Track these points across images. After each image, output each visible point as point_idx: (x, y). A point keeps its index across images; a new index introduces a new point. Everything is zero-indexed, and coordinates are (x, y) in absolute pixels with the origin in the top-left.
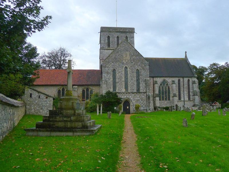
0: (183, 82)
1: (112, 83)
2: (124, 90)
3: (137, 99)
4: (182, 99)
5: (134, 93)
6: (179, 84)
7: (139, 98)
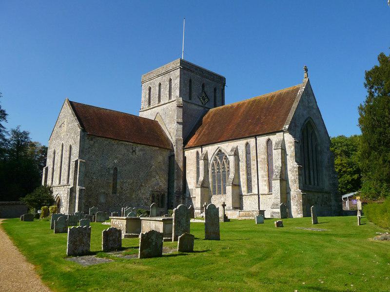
4: (255, 191)
6: (248, 153)
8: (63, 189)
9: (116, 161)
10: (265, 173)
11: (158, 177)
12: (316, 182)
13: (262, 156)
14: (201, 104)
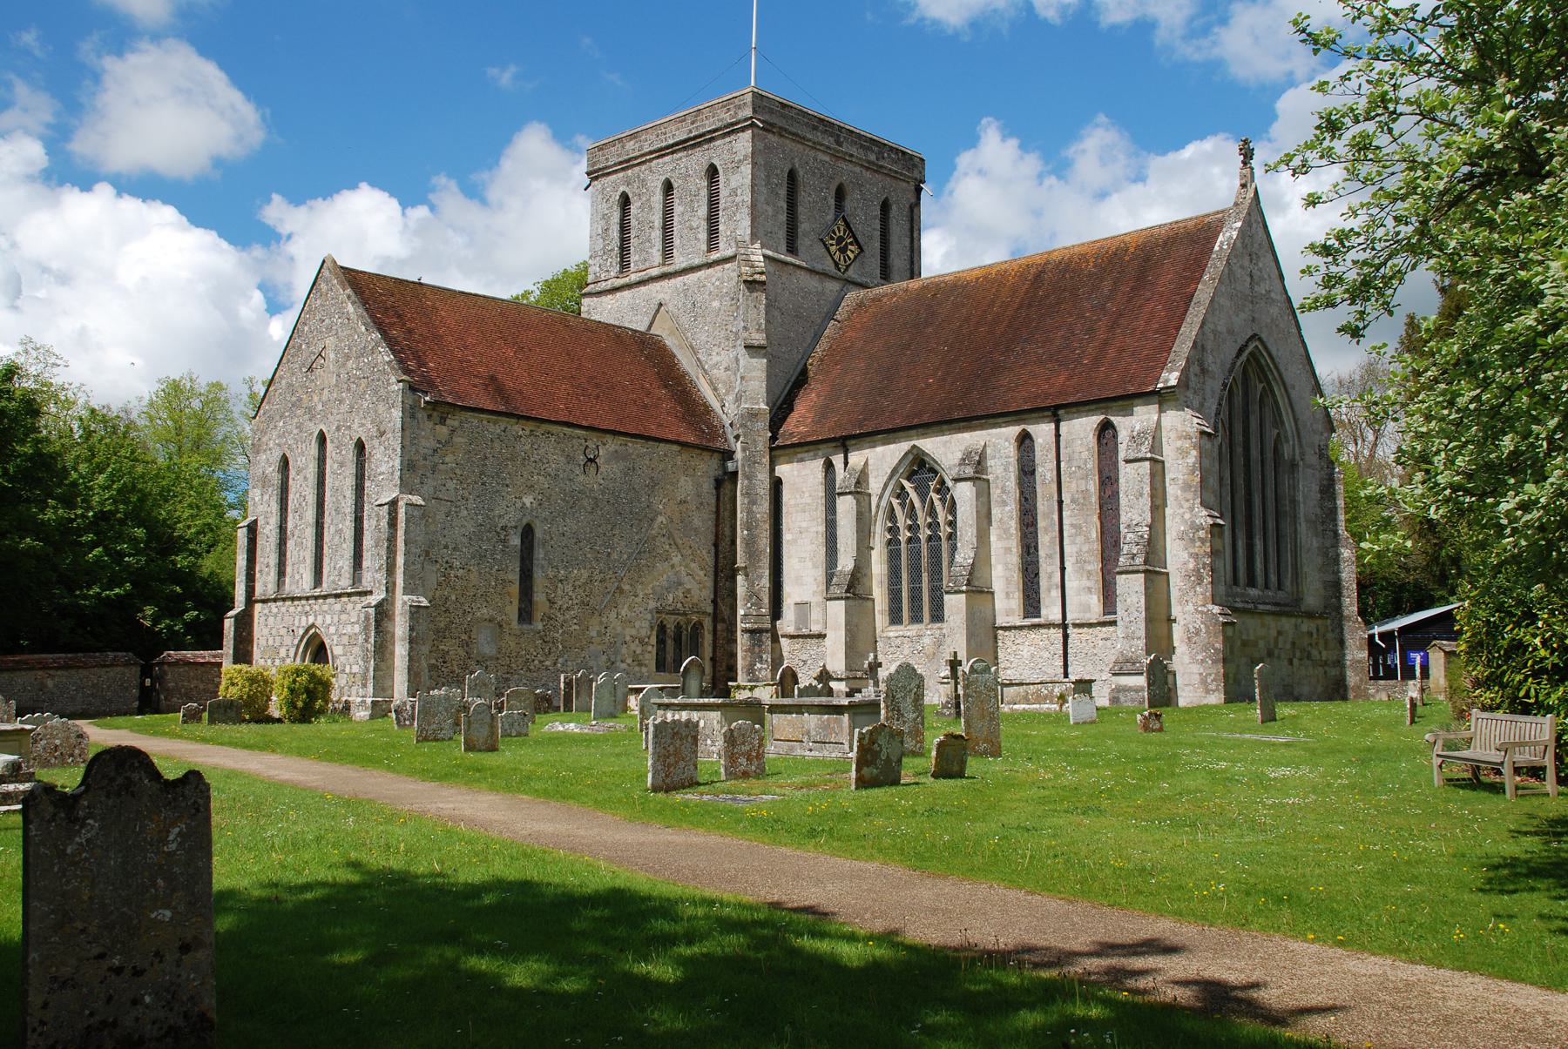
4: (1051, 612)
6: (1027, 471)
8: (338, 607)
9: (528, 500)
10: (1085, 548)
11: (676, 560)
12: (1273, 578)
13: (1082, 484)
14: (831, 268)
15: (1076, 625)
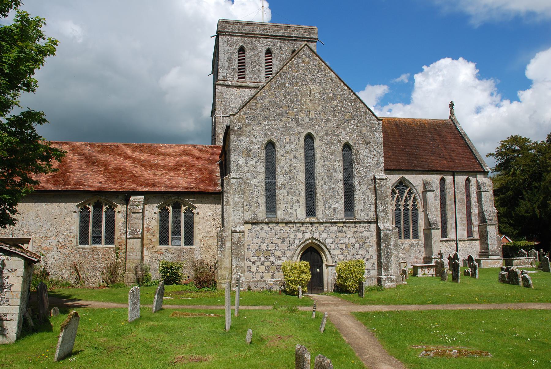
0: (453, 185)
1: (262, 187)
2: (301, 213)
3: (346, 241)
4: (452, 236)
5: (336, 223)
6: (443, 190)
7: (353, 241)
10: (463, 217)
13: (461, 197)
15: (460, 241)
